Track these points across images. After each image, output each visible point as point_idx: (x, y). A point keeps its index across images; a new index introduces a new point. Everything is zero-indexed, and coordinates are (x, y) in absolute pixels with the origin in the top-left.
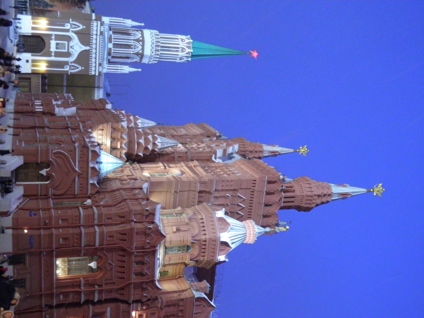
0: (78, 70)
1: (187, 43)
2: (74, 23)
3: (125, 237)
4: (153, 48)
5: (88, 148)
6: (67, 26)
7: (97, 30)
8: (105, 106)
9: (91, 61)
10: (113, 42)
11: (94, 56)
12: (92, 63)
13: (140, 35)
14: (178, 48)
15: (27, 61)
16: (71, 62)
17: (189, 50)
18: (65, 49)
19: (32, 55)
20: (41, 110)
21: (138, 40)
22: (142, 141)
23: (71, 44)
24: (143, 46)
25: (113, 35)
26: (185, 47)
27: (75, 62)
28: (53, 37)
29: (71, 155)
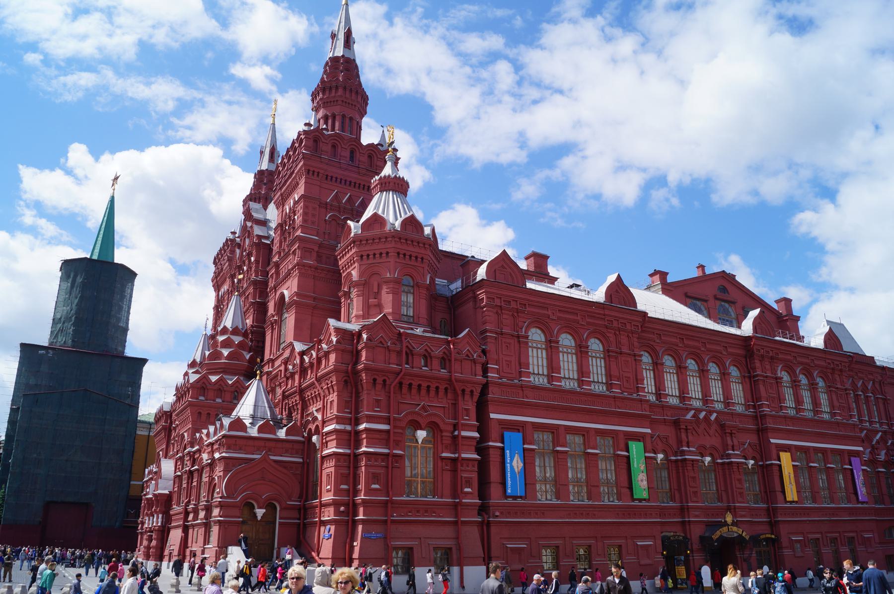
3: (380, 380)
5: (224, 436)
8: (166, 412)
20: (160, 516)
22: (226, 352)
29: (234, 466)
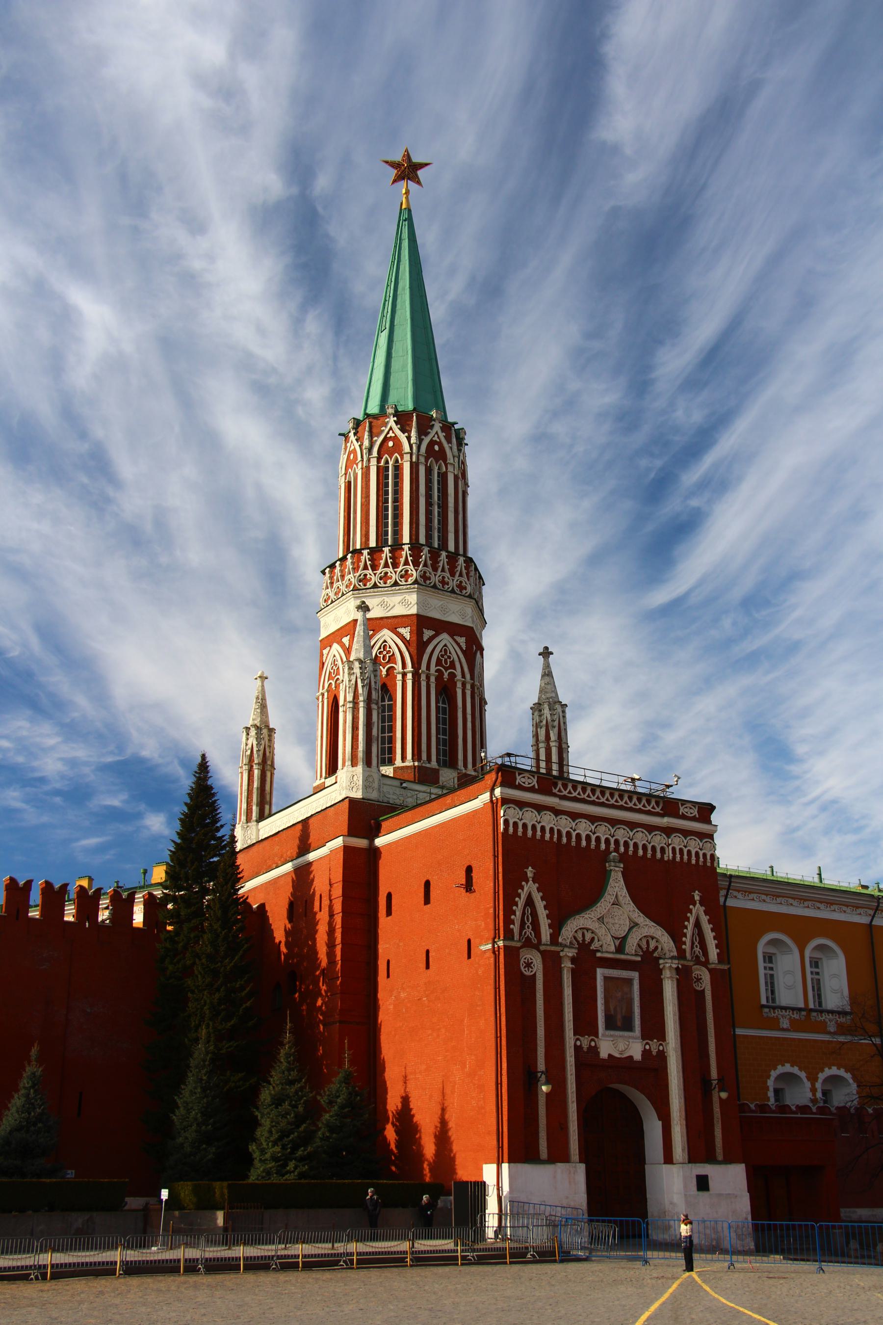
0: (704, 919)
2: (516, 928)
4: (443, 582)
6: (529, 965)
7: (540, 808)
9: (663, 850)
10: (434, 764)
11: (640, 837)
12: (674, 849)
13: (386, 634)
14: (429, 471)
15: (703, 1183)
16: (681, 955)
17: (437, 427)
18: (629, 981)
19: (668, 1159)
21: (418, 647)
23: (606, 946)
24: (441, 626)
26: (426, 441)
27: (677, 936)
28: (585, 1042)
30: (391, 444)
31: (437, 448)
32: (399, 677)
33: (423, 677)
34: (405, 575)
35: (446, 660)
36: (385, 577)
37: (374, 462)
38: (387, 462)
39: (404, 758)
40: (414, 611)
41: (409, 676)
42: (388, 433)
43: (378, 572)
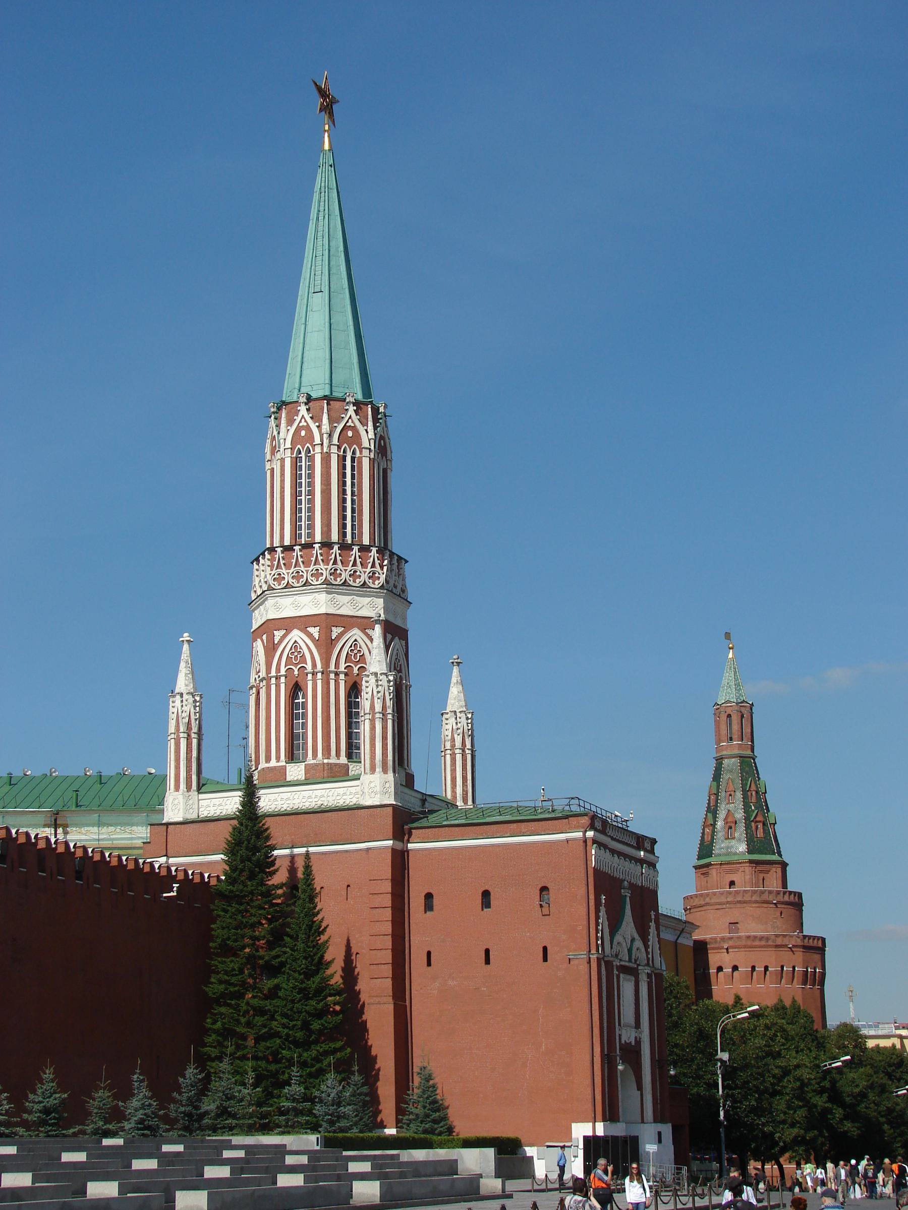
1: (316, 418)
10: (343, 760)
13: (296, 635)
17: (352, 409)
21: (326, 645)
24: (348, 622)
25: (310, 760)
30: (303, 433)
31: (350, 434)
32: (310, 677)
33: (332, 676)
34: (317, 574)
35: (355, 657)
36: (297, 576)
37: (288, 452)
38: (300, 453)
39: (315, 755)
40: (323, 610)
41: (319, 676)
42: (300, 421)
43: (291, 571)
